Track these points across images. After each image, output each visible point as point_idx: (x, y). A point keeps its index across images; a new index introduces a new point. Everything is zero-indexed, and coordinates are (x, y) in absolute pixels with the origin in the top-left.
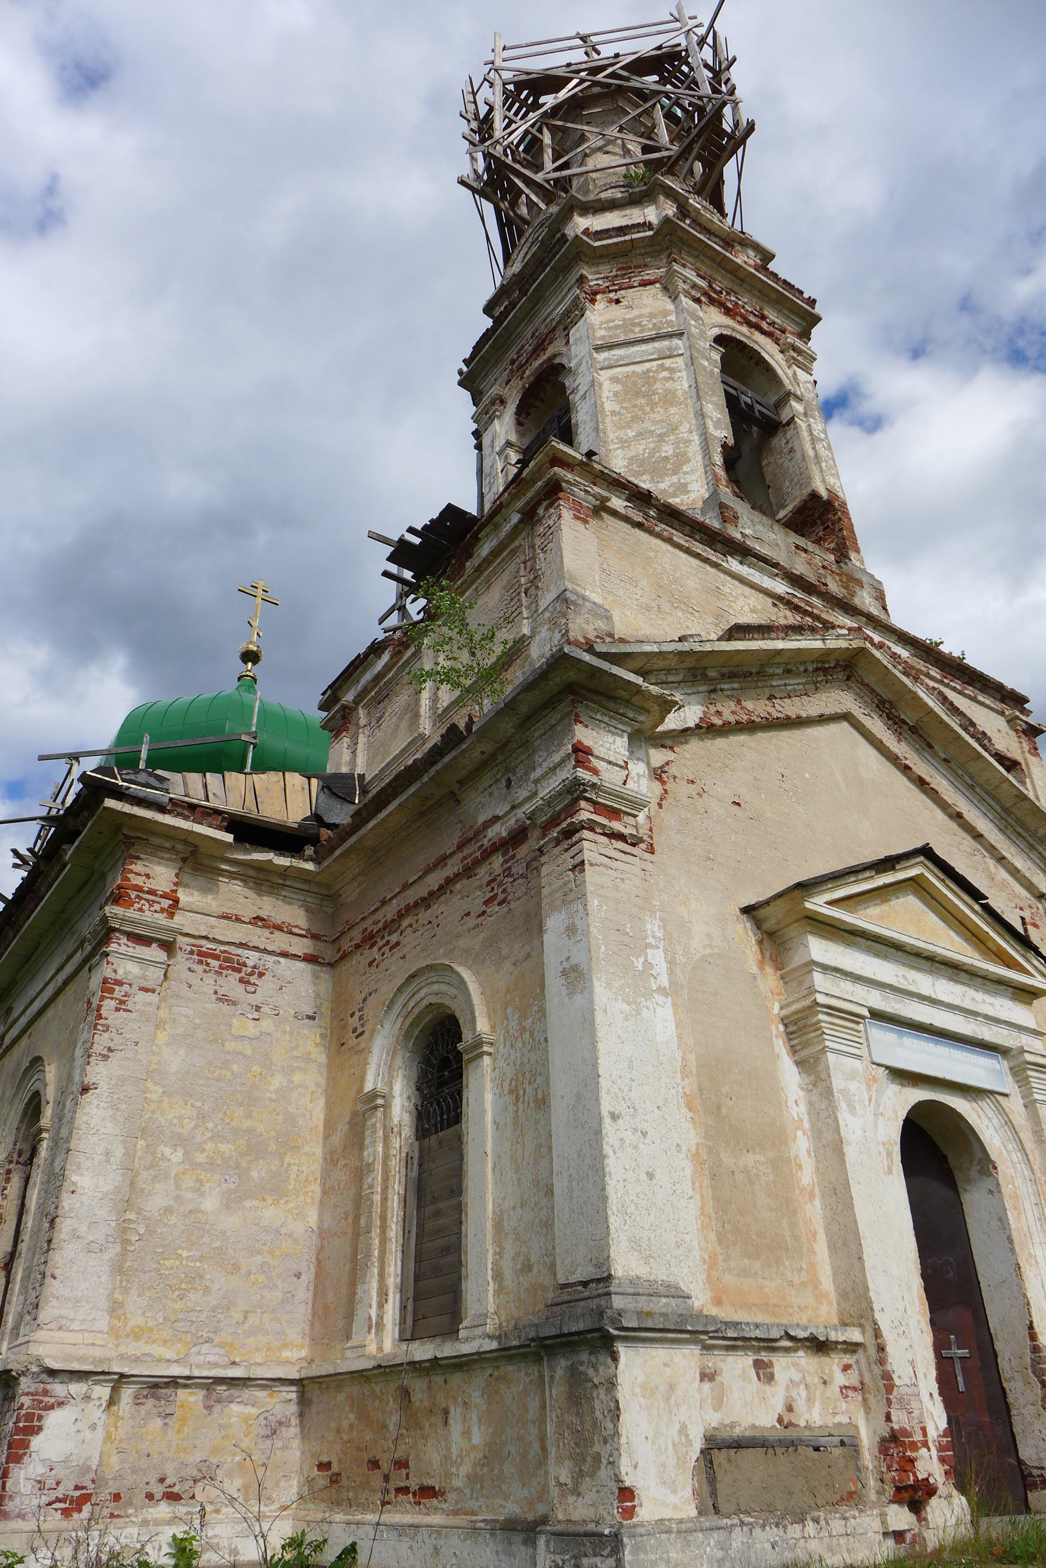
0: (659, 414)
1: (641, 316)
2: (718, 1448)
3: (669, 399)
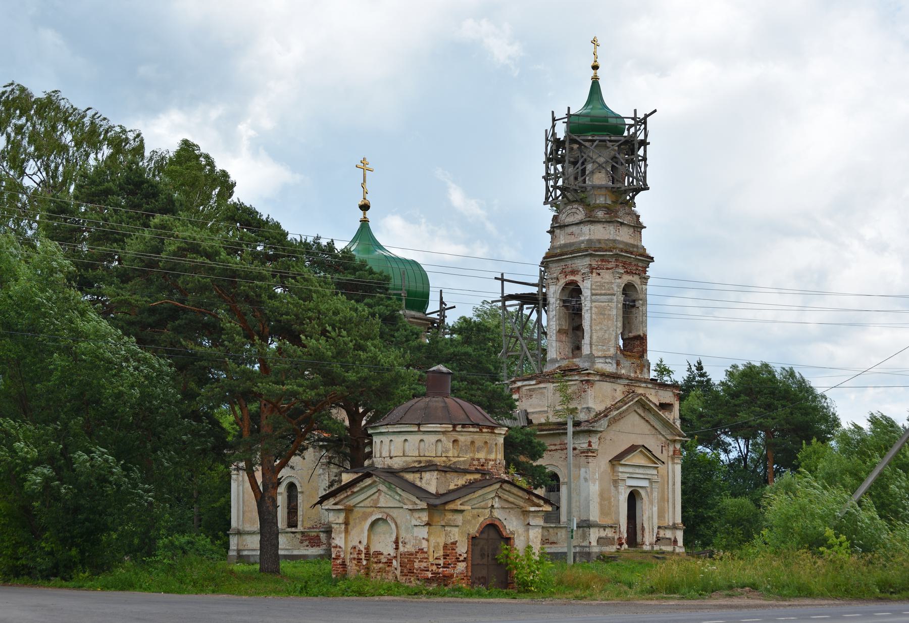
0: (605, 322)
2: (600, 538)
3: (609, 317)
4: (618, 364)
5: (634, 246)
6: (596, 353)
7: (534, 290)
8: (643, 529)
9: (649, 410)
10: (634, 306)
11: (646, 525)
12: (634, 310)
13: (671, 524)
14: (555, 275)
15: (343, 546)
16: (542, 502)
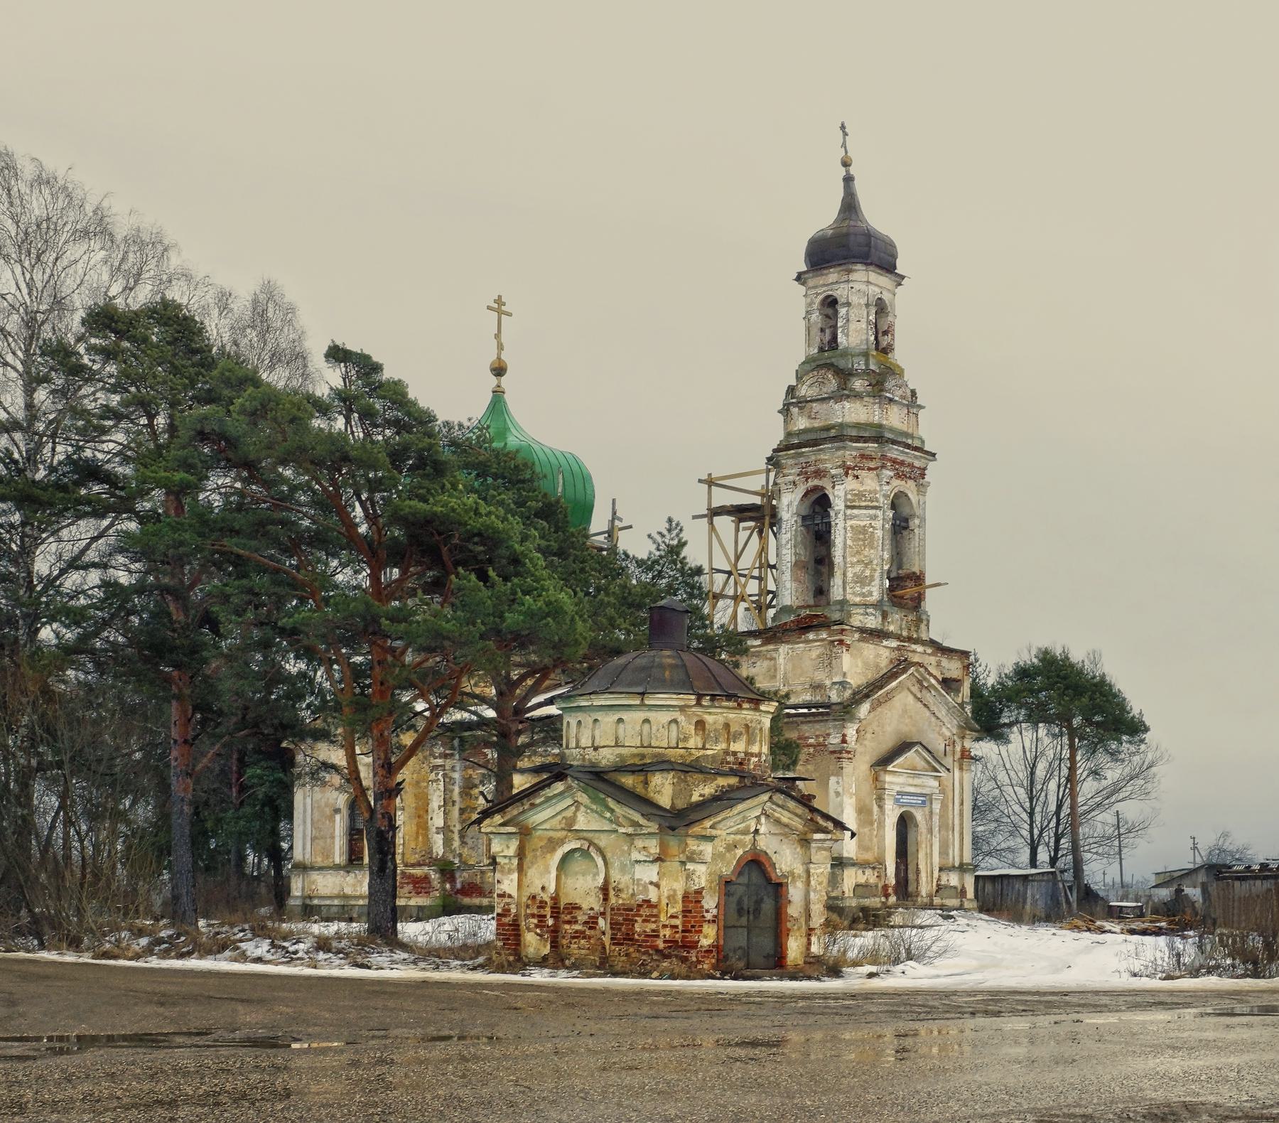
2: (857, 886)
4: (885, 616)
5: (907, 435)
7: (757, 500)
8: (918, 872)
10: (906, 528)
11: (922, 867)
12: (905, 533)
13: (957, 864)
14: (791, 478)
15: (515, 894)
16: (830, 825)
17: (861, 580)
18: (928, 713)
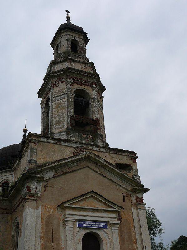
1: (60, 90)
3: (63, 108)
4: (68, 134)
6: (54, 131)
9: (103, 166)
17: (59, 123)
18: (107, 180)
